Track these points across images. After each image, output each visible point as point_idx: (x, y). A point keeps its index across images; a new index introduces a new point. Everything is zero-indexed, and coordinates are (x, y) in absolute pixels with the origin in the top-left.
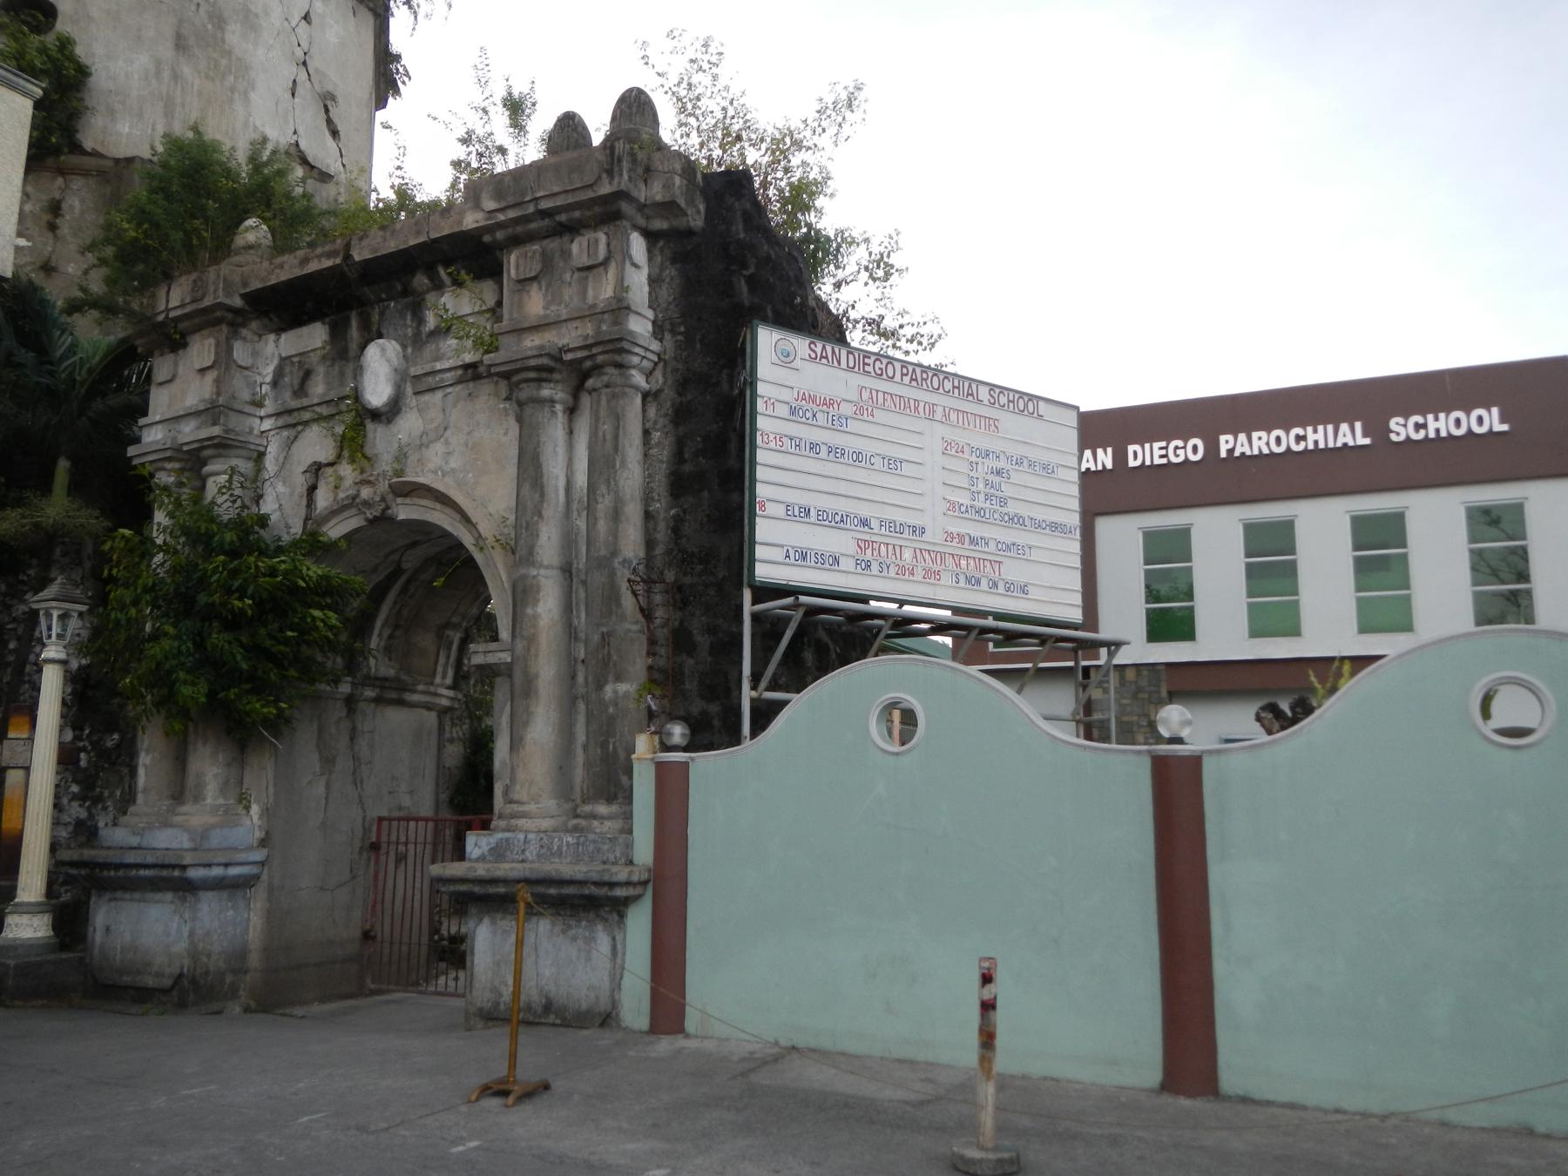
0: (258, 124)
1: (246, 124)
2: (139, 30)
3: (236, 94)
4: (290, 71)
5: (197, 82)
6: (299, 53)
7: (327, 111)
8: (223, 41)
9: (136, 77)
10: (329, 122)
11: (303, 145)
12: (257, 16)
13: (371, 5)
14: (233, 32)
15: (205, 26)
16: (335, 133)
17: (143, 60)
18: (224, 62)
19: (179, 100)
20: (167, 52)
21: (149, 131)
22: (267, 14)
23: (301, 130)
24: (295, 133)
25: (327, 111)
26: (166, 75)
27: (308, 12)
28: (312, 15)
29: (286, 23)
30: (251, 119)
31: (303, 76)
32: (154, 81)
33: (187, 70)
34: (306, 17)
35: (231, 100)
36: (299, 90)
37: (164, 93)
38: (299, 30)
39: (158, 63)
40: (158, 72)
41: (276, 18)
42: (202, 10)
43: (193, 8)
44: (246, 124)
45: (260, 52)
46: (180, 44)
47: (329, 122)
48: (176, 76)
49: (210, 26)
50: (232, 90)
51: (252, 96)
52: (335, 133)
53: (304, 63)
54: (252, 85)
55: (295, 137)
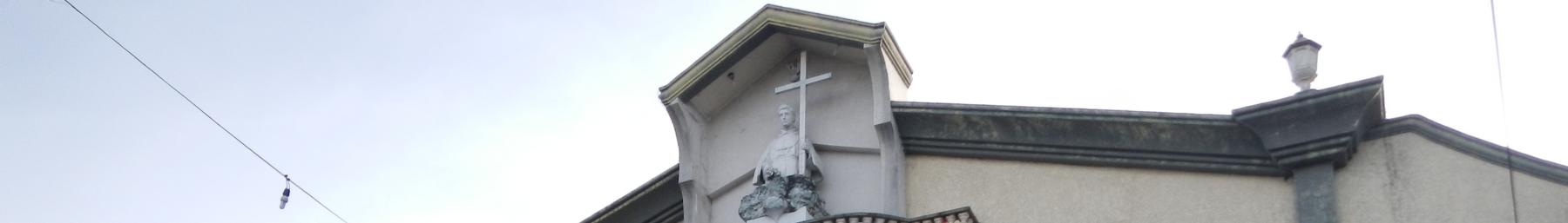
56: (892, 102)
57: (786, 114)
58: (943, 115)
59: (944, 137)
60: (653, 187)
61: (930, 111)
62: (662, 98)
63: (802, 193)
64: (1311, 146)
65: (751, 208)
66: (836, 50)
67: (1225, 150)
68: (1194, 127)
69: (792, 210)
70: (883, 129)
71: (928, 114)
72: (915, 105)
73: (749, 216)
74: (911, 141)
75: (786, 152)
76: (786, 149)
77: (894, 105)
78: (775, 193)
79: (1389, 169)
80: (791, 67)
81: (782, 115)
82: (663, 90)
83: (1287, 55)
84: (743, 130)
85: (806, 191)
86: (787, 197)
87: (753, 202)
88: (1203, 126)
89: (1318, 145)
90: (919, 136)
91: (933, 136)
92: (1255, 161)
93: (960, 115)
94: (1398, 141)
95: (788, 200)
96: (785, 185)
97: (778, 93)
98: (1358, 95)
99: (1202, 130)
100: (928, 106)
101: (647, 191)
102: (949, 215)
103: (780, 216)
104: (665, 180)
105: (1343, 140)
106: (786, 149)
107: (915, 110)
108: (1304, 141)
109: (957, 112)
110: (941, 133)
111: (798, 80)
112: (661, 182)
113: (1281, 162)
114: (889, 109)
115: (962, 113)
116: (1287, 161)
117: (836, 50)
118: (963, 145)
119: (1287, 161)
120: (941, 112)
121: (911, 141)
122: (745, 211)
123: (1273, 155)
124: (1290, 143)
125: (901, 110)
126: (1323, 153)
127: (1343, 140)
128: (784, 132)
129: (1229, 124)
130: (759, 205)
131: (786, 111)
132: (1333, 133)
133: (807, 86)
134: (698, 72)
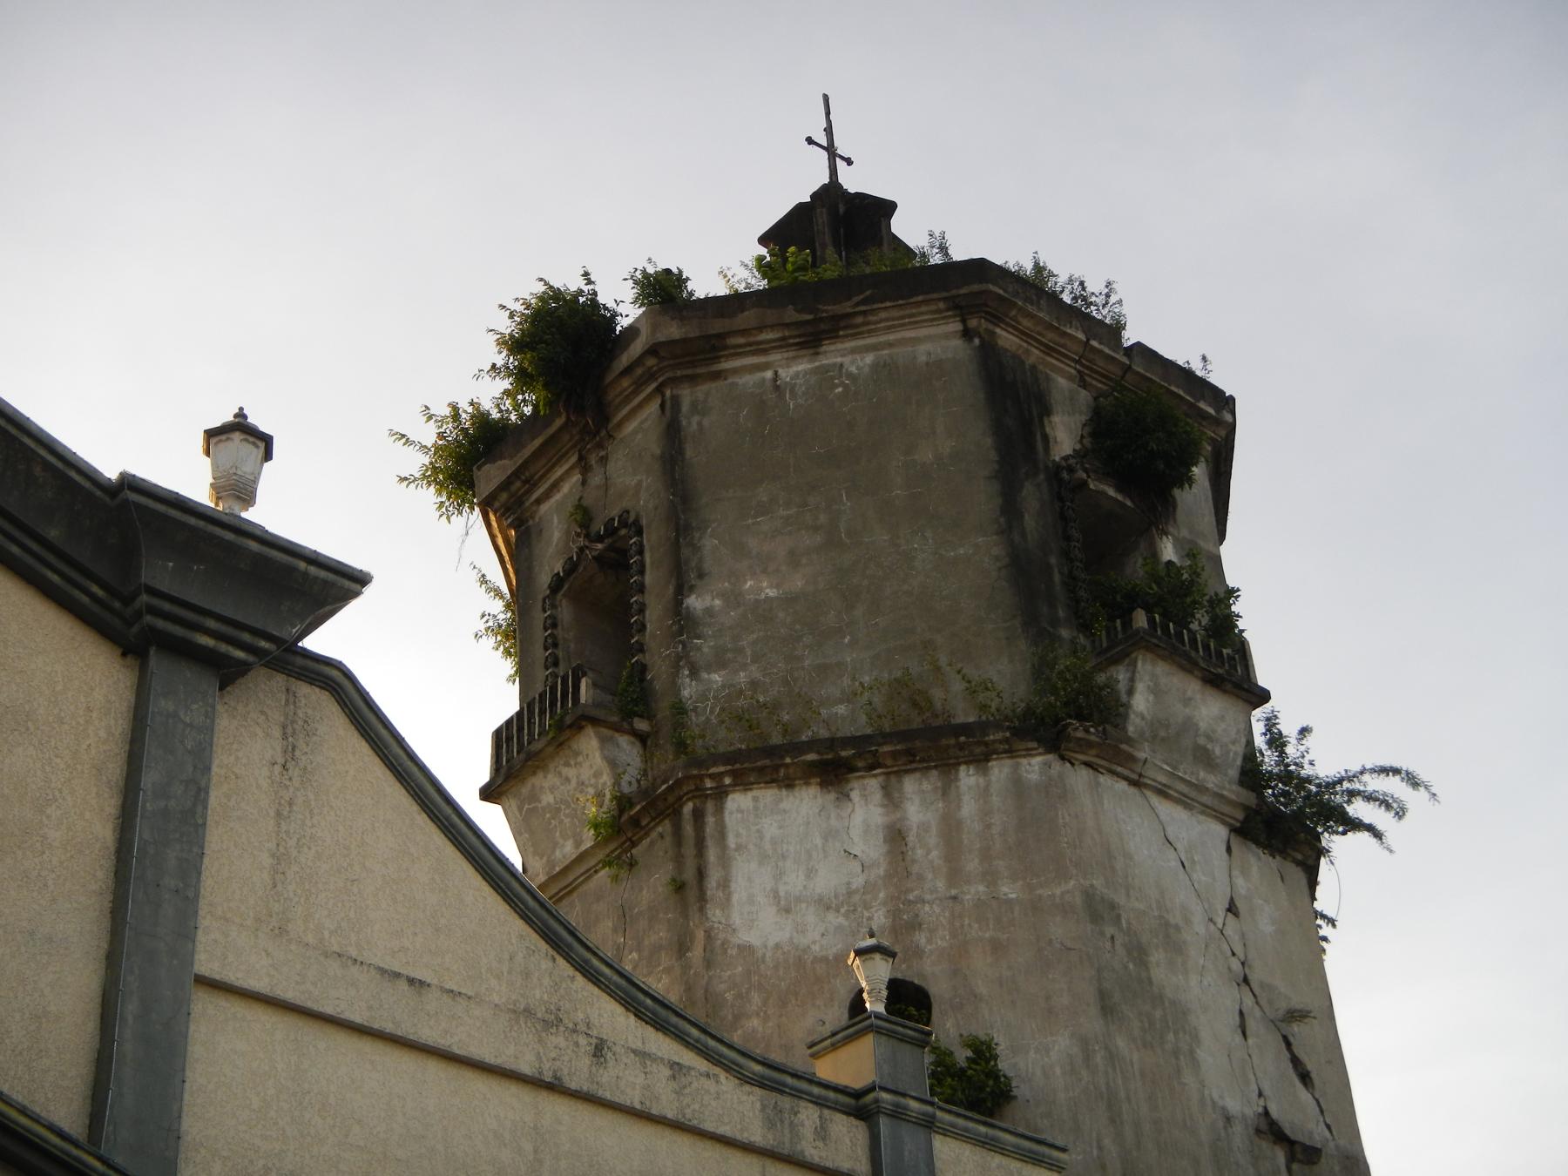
0: (1216, 1096)
1: (1202, 1101)
2: (1048, 998)
3: (1182, 1057)
4: (1229, 998)
5: (1136, 1057)
6: (1235, 965)
7: (1288, 1044)
8: (1150, 980)
9: (1058, 1071)
10: (1296, 1062)
11: (1274, 1114)
12: (1177, 928)
13: (1299, 857)
14: (1158, 964)
15: (1126, 968)
16: (1305, 1078)
17: (1062, 1044)
18: (1158, 1014)
19: (1122, 1094)
20: (1092, 1023)
21: (1095, 1152)
22: (1188, 921)
23: (1267, 1091)
24: (1260, 1095)
25: (1288, 1044)
26: (1099, 1058)
27: (1232, 901)
28: (1239, 904)
29: (1212, 926)
30: (1206, 1092)
31: (1249, 1001)
32: (1084, 1073)
33: (1121, 1043)
34: (1232, 909)
35: (1179, 1071)
36: (1251, 1025)
37: (1103, 1088)
38: (1229, 931)
39: (1085, 1043)
40: (1088, 1057)
41: (1199, 926)
42: (1118, 943)
43: (1108, 945)
44: (1202, 1101)
45: (1194, 980)
46: (1107, 1009)
47: (1296, 1062)
48: (1112, 1057)
49: (1131, 966)
50: (1176, 1053)
51: (1201, 1054)
52: (1305, 1078)
53: (1246, 980)
54: (1195, 1038)
55: (1262, 1102)
64: (211, 624)
67: (53, 534)
68: (30, 456)
79: (285, 734)
83: (213, 435)
88: (47, 466)
89: (223, 628)
92: (95, 589)
94: (304, 690)
98: (325, 582)
99: (38, 470)
105: (263, 644)
108: (207, 607)
113: (148, 619)
116: (160, 624)
119: (160, 624)
123: (144, 598)
124: (182, 596)
126: (224, 648)
127: (263, 644)
129: (99, 493)
132: (258, 624)
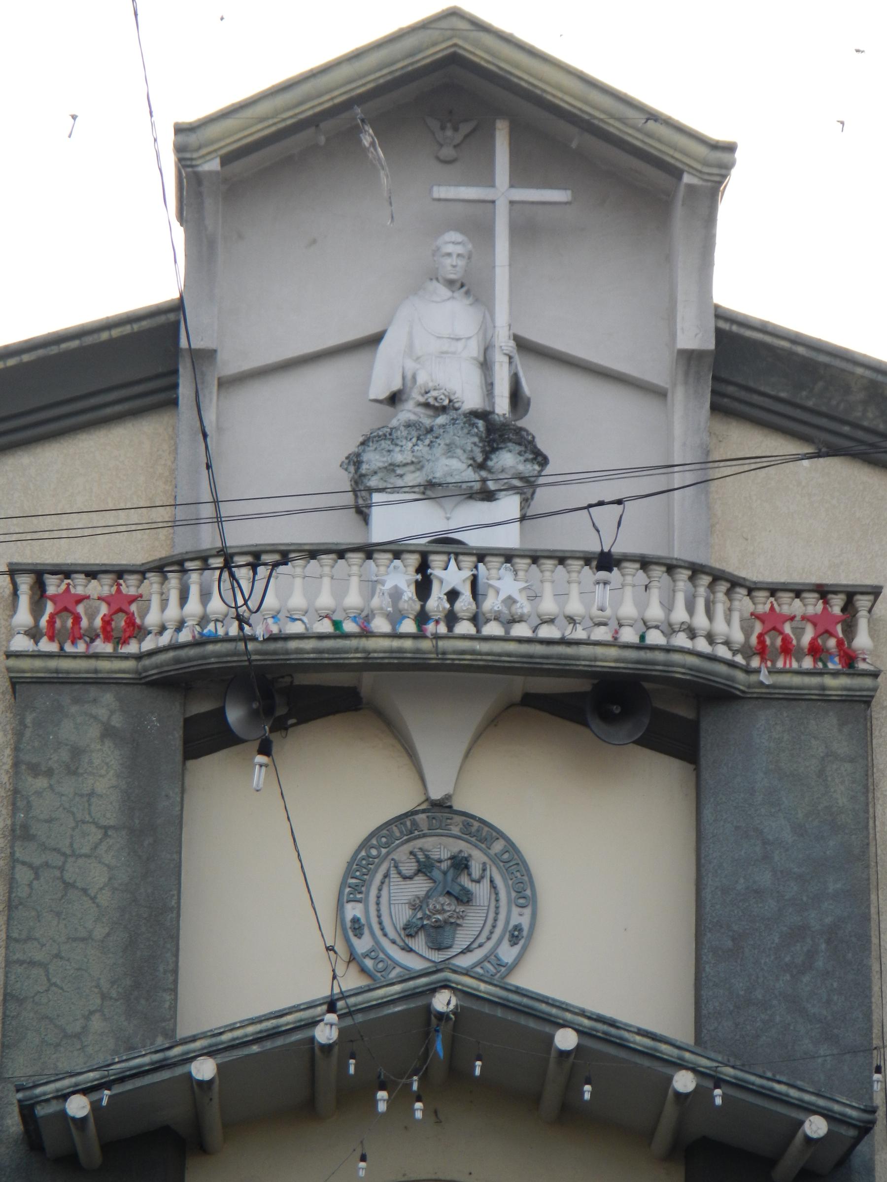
56: (717, 307)
57: (459, 255)
58: (827, 366)
59: (810, 403)
60: (105, 336)
61: (800, 350)
62: (180, 149)
63: (521, 467)
65: (391, 468)
66: (577, 139)
69: (488, 496)
70: (689, 357)
71: (792, 354)
72: (769, 329)
73: (382, 485)
74: (731, 389)
75: (460, 345)
76: (458, 339)
77: (720, 314)
78: (459, 452)
80: (443, 128)
81: (449, 255)
82: (180, 130)
84: (314, 242)
85: (529, 466)
86: (482, 466)
87: (399, 458)
90: (751, 384)
91: (783, 395)
93: (862, 377)
95: (484, 474)
96: (481, 440)
97: (439, 200)
100: (797, 339)
101: (88, 340)
102: (835, 593)
103: (457, 504)
104: (136, 327)
106: (458, 339)
107: (768, 339)
109: (859, 371)
110: (804, 393)
111: (491, 183)
112: (127, 329)
114: (711, 324)
115: (868, 373)
117: (577, 139)
118: (846, 429)
120: (822, 358)
121: (731, 389)
122: (376, 473)
125: (735, 328)
128: (444, 291)
130: (411, 468)
131: (459, 249)
133: (512, 203)
134: (276, 113)
